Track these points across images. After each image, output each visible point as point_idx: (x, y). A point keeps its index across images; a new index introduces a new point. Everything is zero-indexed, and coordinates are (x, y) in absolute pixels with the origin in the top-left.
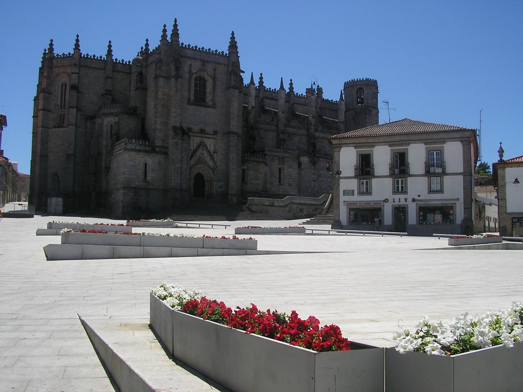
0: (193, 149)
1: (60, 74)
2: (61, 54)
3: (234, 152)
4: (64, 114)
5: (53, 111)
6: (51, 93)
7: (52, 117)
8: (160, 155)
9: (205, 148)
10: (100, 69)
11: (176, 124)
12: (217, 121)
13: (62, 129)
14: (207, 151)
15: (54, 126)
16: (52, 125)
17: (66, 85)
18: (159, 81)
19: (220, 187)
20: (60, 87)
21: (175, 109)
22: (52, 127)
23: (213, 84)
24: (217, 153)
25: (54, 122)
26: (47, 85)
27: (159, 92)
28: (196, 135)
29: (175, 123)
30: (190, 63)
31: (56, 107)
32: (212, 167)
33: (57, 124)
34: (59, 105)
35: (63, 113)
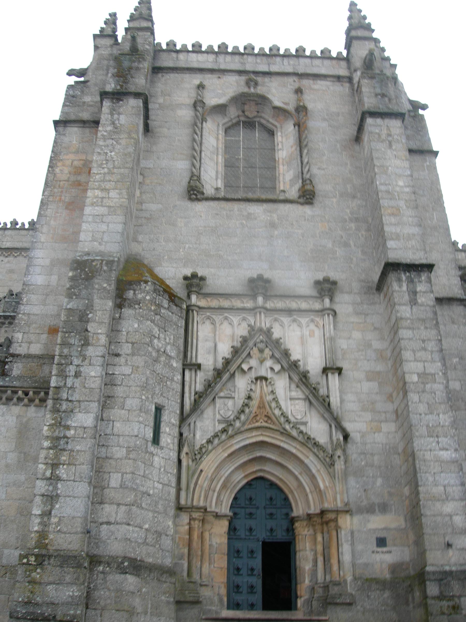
0: (215, 360)
3: (425, 349)
8: (26, 394)
9: (277, 355)
11: (100, 244)
12: (330, 245)
14: (285, 365)
18: (64, 135)
19: (381, 542)
21: (98, 193)
23: (297, 127)
24: (339, 371)
27: (59, 164)
28: (226, 303)
29: (94, 240)
30: (197, 82)
32: (322, 439)
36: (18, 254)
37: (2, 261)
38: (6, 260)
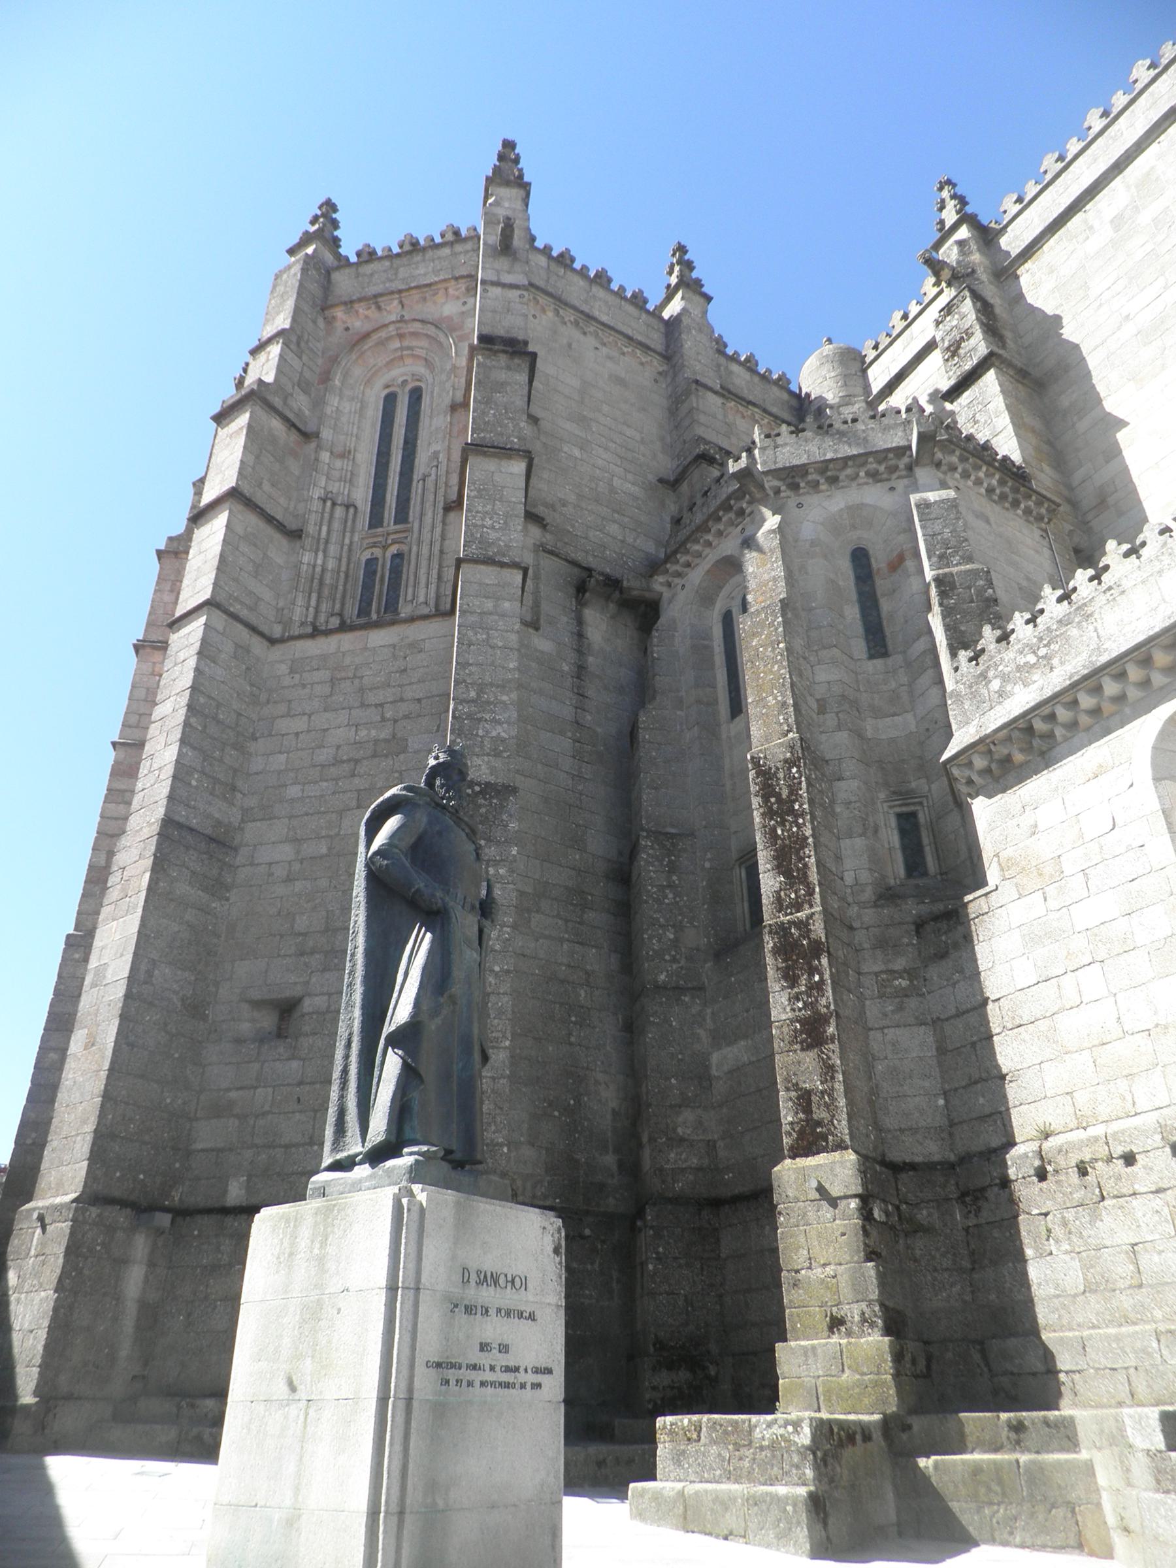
1: (383, 334)
2: (386, 239)
4: (399, 556)
5: (311, 529)
6: (307, 436)
7: (305, 567)
10: (646, 348)
13: (379, 638)
15: (315, 629)
16: (296, 618)
17: (419, 398)
20: (374, 413)
22: (296, 631)
25: (313, 603)
26: (280, 371)
31: (339, 512)
33: (341, 615)
34: (365, 507)
35: (394, 549)
36: (630, 350)
37: (597, 348)
38: (605, 350)
